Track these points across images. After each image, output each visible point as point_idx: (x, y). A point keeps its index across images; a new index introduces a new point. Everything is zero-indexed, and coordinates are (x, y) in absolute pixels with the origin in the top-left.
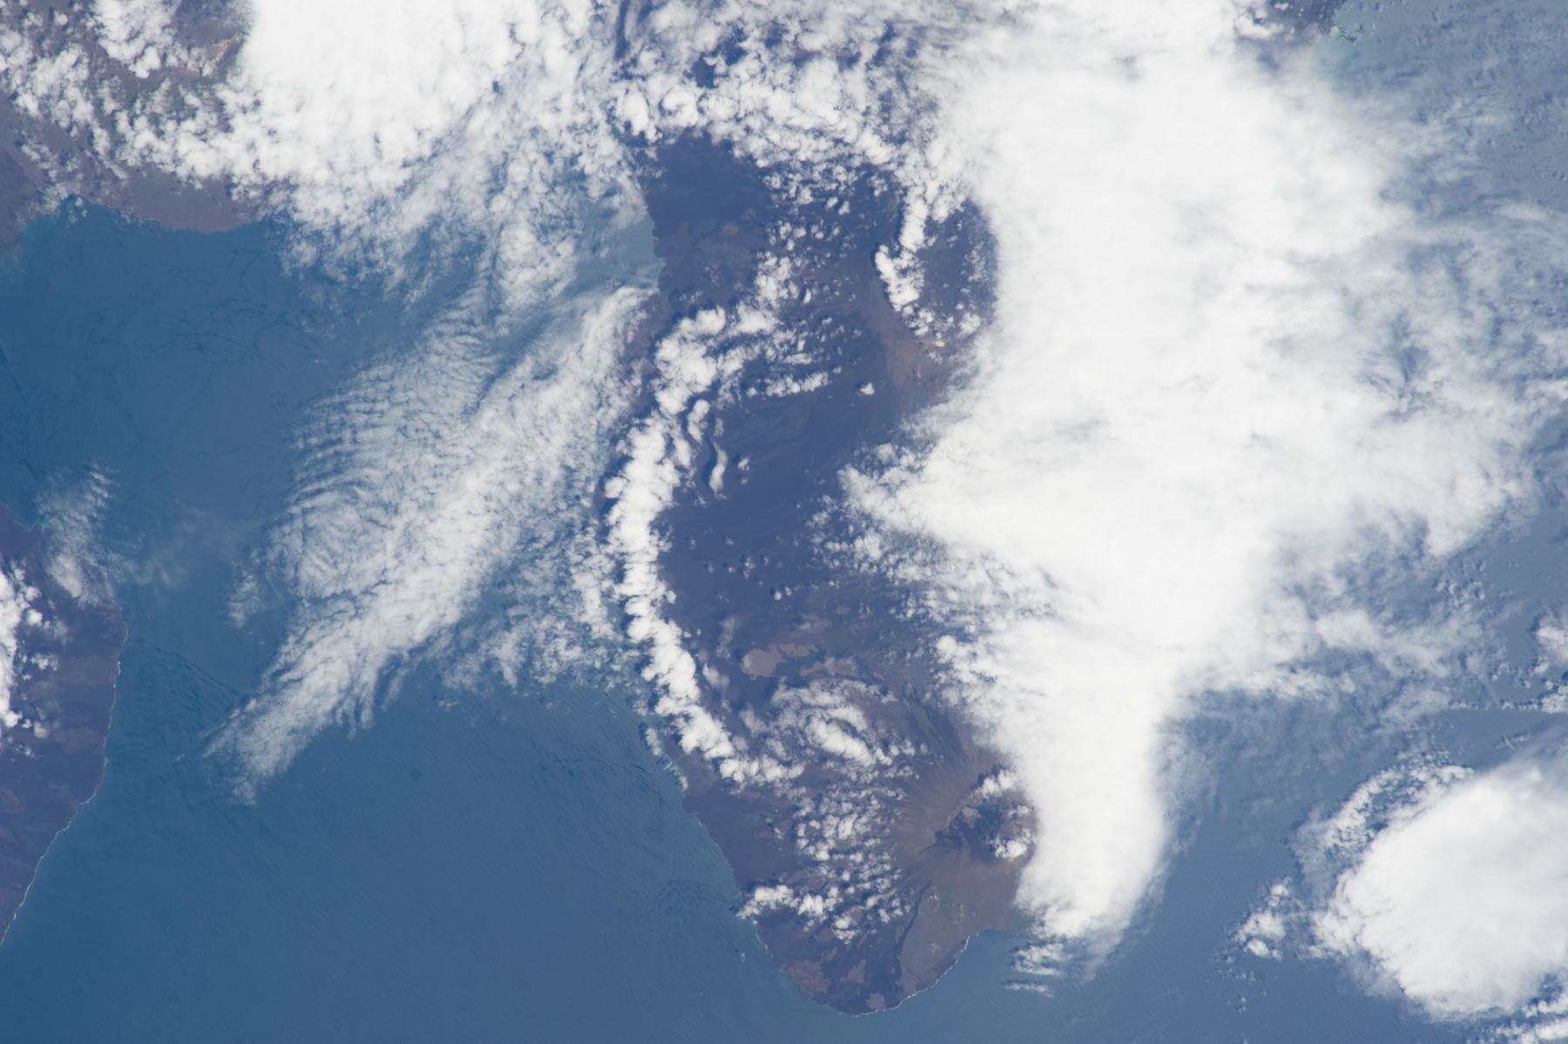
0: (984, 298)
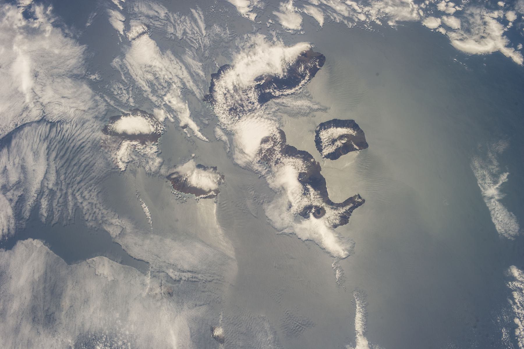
0: (261, 76)
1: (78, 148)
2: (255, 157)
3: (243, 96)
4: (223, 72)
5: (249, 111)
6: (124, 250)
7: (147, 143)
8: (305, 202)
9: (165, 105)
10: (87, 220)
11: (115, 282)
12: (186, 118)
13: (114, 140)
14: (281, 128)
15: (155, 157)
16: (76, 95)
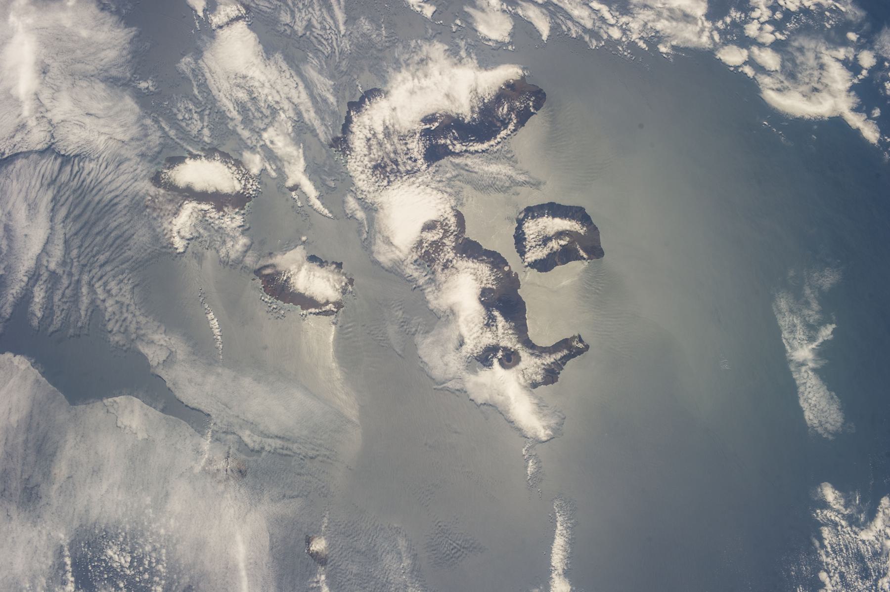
0: (433, 115)
1: (106, 205)
2: (409, 254)
3: (398, 146)
4: (369, 100)
5: (408, 172)
6: (169, 389)
7: (226, 209)
8: (488, 339)
9: (264, 146)
10: (110, 332)
11: (148, 442)
12: (297, 174)
13: (169, 197)
14: (459, 208)
15: (237, 234)
16: (111, 113)
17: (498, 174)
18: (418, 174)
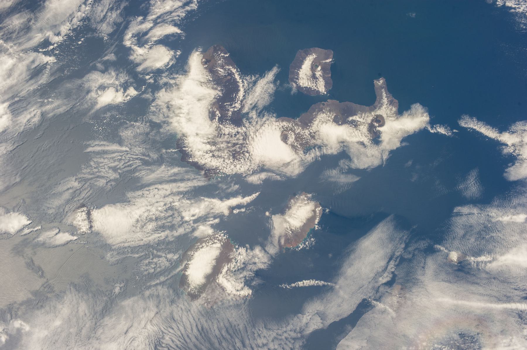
0: (210, 112)
2: (298, 155)
4: (185, 147)
5: (244, 139)
7: (232, 257)
8: (364, 129)
9: (196, 221)
12: (222, 206)
13: (210, 291)
15: (251, 254)
17: (263, 88)
18: (248, 134)
